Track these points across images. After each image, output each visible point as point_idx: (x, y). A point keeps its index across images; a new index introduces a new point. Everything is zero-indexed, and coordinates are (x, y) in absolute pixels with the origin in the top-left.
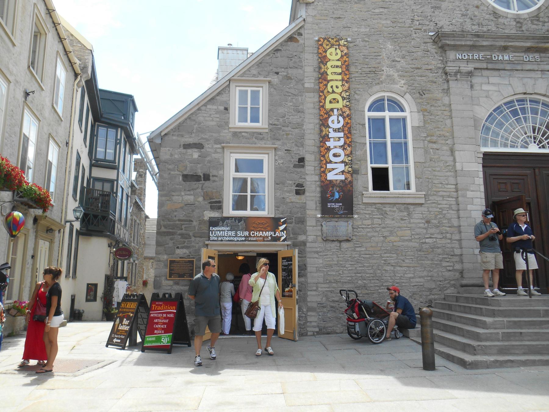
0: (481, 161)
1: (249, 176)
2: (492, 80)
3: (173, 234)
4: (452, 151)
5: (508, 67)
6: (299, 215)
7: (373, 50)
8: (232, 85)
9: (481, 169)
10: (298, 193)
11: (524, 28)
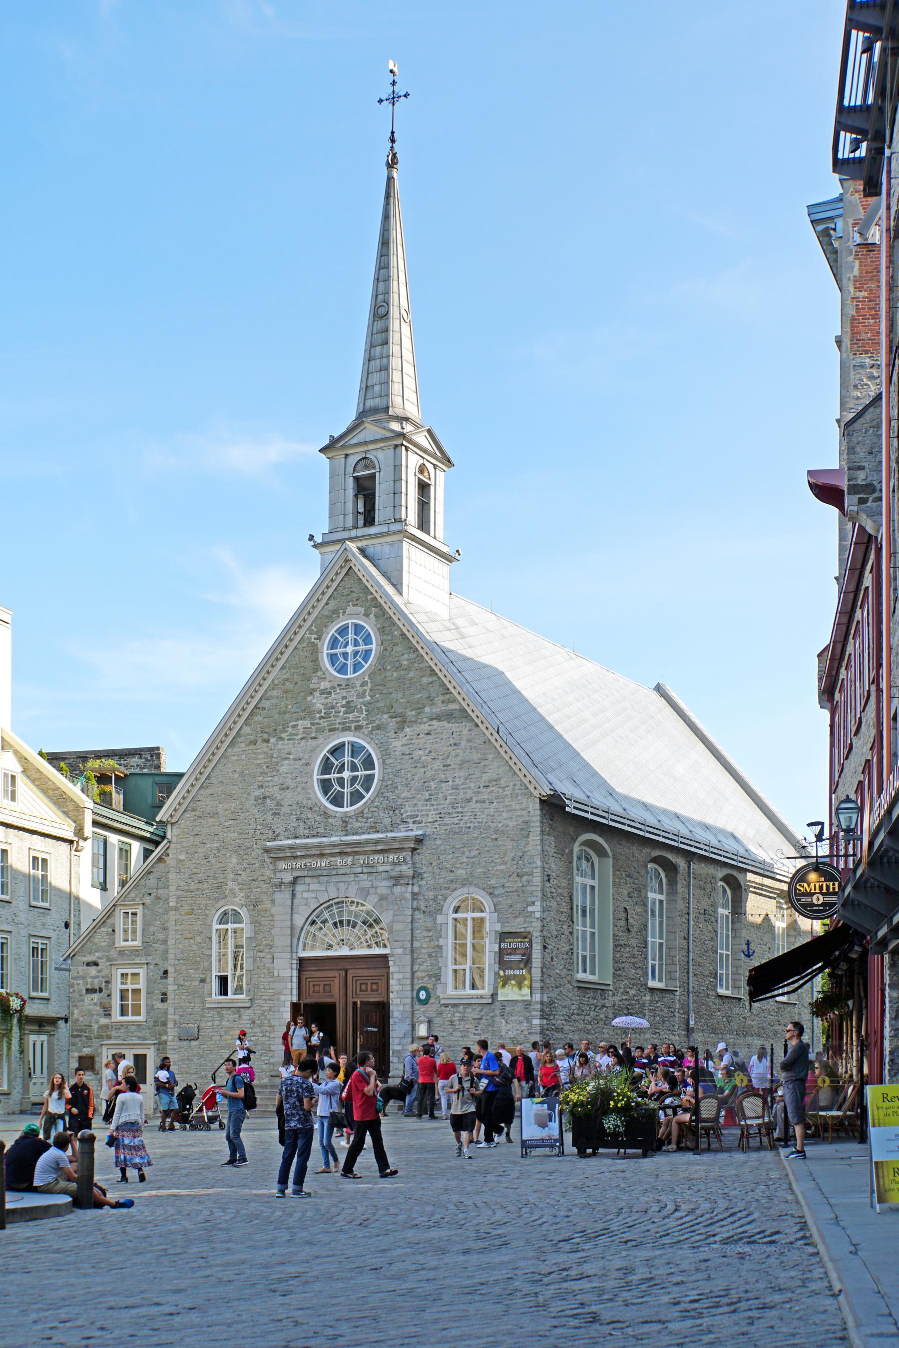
0: (294, 966)
2: (312, 887)
3: (81, 1036)
4: (273, 958)
5: (325, 873)
6: (163, 1019)
7: (221, 865)
8: (117, 909)
9: (295, 973)
10: (163, 1000)
11: (348, 828)
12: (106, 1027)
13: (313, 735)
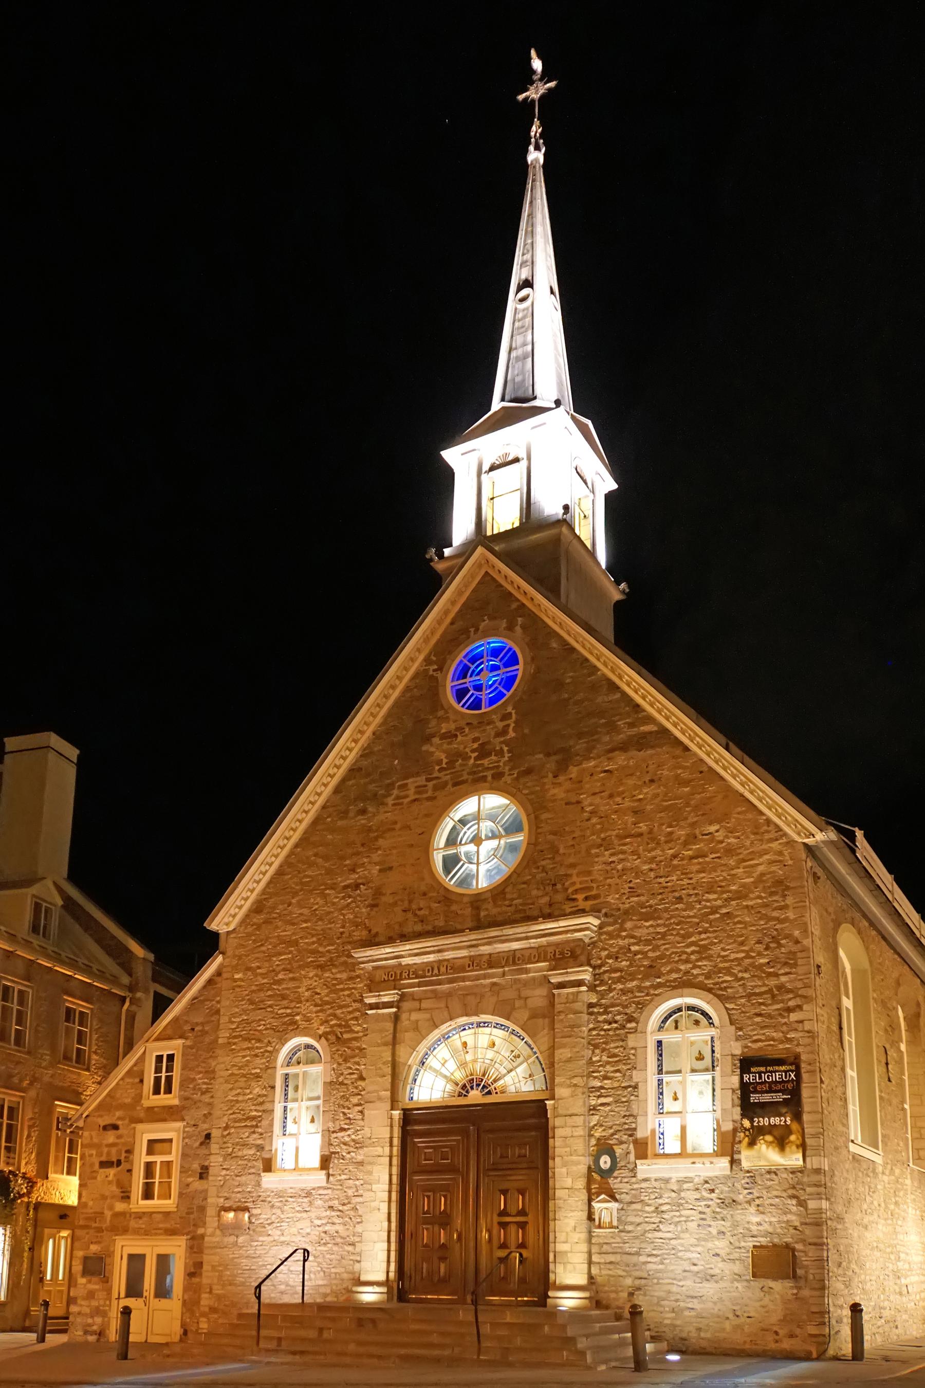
1: (158, 1159)
12: (123, 1214)
13: (430, 794)
